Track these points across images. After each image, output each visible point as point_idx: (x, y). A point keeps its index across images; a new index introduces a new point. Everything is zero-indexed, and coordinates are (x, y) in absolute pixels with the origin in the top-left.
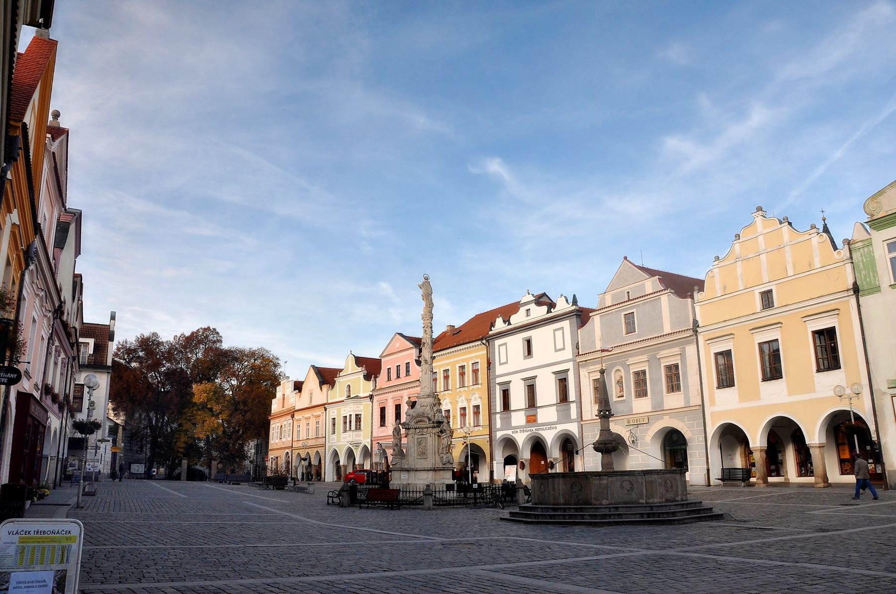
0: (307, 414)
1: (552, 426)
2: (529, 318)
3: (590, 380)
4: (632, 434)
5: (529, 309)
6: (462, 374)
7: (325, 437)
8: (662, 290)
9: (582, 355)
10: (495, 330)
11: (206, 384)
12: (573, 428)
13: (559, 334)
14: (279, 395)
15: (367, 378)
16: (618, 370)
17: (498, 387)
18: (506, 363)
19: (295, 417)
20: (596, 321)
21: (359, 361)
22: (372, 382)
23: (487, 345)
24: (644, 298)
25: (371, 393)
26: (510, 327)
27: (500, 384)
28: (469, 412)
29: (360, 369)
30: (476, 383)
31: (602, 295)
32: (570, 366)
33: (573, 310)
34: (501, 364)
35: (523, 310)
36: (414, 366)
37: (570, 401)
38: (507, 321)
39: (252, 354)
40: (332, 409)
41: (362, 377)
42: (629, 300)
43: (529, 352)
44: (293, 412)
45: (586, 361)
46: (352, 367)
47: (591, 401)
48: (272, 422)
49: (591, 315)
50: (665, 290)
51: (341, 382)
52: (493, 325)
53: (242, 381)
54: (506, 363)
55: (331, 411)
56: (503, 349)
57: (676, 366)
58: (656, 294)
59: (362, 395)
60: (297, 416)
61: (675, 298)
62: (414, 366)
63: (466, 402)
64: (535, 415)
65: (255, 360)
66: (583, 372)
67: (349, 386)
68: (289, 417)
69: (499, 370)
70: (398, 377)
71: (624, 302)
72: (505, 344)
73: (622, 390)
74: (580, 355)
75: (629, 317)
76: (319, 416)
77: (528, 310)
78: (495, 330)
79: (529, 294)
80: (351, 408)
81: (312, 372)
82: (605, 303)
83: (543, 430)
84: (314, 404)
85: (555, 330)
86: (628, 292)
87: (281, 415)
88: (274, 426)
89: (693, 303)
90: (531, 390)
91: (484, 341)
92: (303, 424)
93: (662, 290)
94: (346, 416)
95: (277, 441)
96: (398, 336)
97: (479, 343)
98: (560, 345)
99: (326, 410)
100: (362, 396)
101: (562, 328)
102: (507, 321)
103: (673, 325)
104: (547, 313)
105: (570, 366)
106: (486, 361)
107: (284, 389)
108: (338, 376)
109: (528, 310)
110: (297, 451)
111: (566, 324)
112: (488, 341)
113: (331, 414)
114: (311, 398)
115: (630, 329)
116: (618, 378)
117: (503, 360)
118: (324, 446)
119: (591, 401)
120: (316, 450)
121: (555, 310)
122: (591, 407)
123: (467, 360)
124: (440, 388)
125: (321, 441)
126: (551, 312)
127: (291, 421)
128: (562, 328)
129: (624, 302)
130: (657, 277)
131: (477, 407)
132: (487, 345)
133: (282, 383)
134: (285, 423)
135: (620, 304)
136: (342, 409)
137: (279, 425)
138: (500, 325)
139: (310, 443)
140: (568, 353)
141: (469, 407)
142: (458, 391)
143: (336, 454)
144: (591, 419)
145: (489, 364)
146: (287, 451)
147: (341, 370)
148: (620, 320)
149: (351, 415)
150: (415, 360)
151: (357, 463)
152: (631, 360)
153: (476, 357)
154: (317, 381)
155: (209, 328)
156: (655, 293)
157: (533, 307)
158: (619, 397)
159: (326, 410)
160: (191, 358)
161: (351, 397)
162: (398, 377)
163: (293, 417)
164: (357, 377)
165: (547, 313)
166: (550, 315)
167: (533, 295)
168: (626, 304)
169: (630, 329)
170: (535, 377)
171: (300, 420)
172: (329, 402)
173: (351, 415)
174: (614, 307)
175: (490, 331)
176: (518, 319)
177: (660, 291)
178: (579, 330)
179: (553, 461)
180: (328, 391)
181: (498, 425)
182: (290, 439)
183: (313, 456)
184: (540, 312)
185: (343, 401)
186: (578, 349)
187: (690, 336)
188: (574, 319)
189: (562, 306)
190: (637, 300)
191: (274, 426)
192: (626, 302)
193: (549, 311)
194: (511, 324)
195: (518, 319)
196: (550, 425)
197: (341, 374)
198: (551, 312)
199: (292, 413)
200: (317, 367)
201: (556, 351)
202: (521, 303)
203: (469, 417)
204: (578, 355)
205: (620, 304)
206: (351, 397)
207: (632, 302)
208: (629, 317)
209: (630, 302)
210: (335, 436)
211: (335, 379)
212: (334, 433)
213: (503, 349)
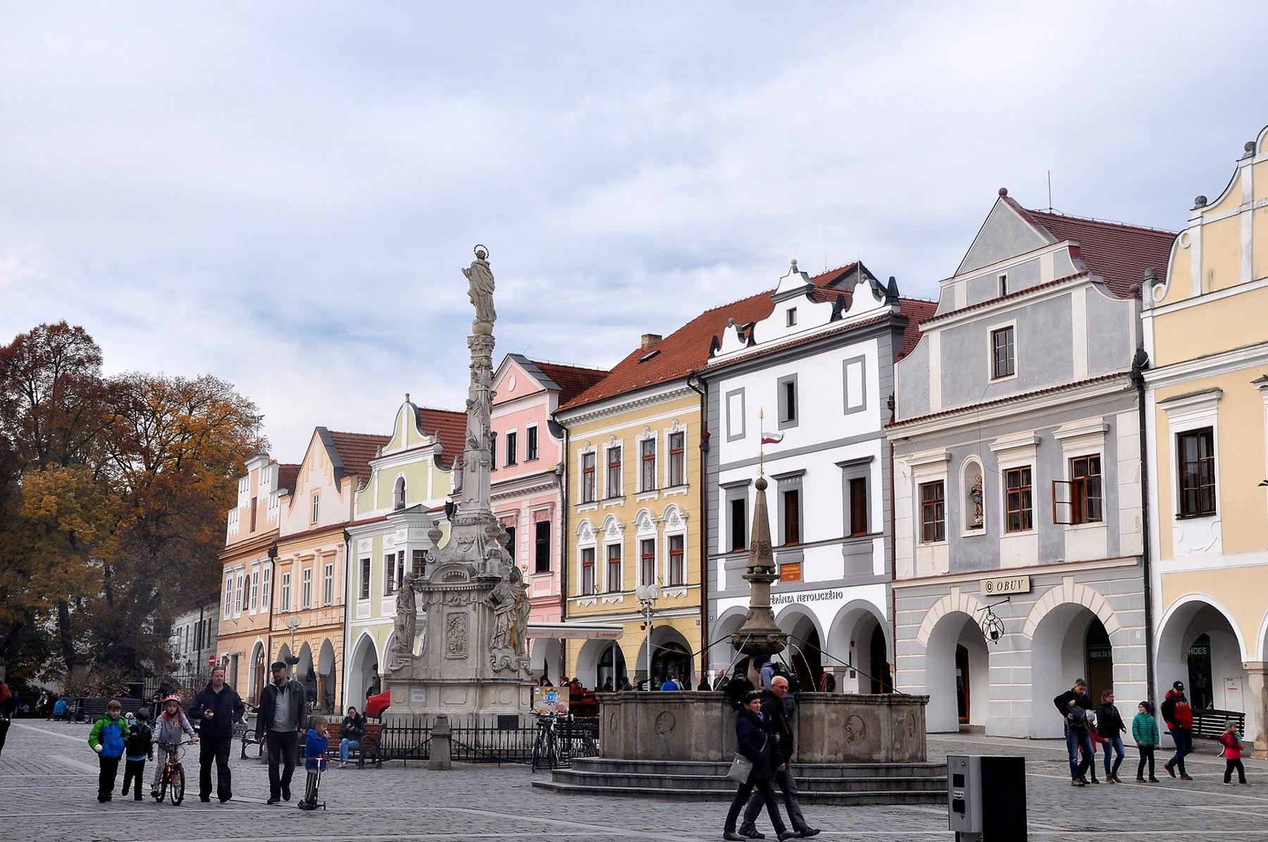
0: (307, 549)
1: (833, 590)
2: (793, 329)
3: (913, 484)
4: (991, 618)
5: (795, 309)
6: (648, 459)
7: (345, 606)
8: (1075, 277)
9: (903, 423)
10: (721, 356)
11: (55, 470)
12: (876, 596)
13: (855, 369)
14: (244, 500)
15: (442, 461)
16: (974, 466)
17: (722, 492)
18: (743, 436)
19: (279, 556)
20: (933, 343)
21: (427, 419)
22: (453, 473)
23: (704, 392)
24: (1036, 294)
25: (450, 500)
26: (753, 350)
27: (728, 486)
28: (661, 552)
29: (426, 440)
30: (676, 482)
31: (948, 282)
32: (873, 448)
33: (883, 316)
34: (730, 439)
35: (781, 309)
36: (545, 435)
37: (873, 532)
38: (746, 334)
39: (187, 393)
40: (361, 536)
41: (430, 458)
42: (1005, 297)
43: (790, 413)
44: (274, 543)
45: (906, 438)
46: (408, 435)
47: (915, 535)
48: (227, 568)
49: (922, 328)
50: (1080, 275)
51: (385, 471)
52: (716, 344)
53: (157, 464)
54: (743, 436)
55: (361, 542)
56: (736, 401)
57: (1095, 460)
58: (1063, 286)
59: (430, 503)
60: (284, 554)
61: (1104, 297)
62: (545, 435)
63: (654, 526)
64: (799, 564)
65: (192, 409)
66: (902, 466)
67: (402, 483)
68: (265, 556)
69: (727, 452)
70: (511, 461)
71: (993, 301)
72: (741, 391)
73: (979, 514)
74: (898, 424)
75: (1001, 337)
76: (334, 553)
77: (791, 312)
78: (721, 356)
79: (796, 271)
80: (401, 535)
81: (319, 442)
82: (952, 300)
83: (814, 598)
84: (322, 523)
85: (846, 363)
86: (1004, 278)
87: (247, 550)
88: (230, 576)
89: (1140, 310)
90: (792, 501)
91: (695, 383)
92: (296, 571)
93: (1075, 277)
94: (393, 556)
95: (237, 615)
96: (513, 363)
97: (684, 386)
98: (855, 400)
99: (347, 537)
100: (432, 507)
101: (861, 359)
102: (746, 334)
103: (1093, 361)
104: (832, 320)
105: (873, 448)
106: (699, 432)
107: (255, 488)
108: (377, 456)
109: (791, 312)
110: (282, 641)
111: (870, 348)
112: (704, 383)
113: (360, 549)
114: (316, 508)
115: (1002, 368)
116: (973, 483)
117: (736, 429)
118: (343, 626)
119: (915, 535)
120: (324, 636)
121: (850, 313)
122: (915, 549)
123: (660, 425)
124: (600, 491)
125: (336, 616)
126: (841, 318)
127: (269, 566)
128: (861, 359)
129: (993, 301)
130: (1067, 243)
131: (677, 540)
132: (704, 392)
133: (250, 469)
134: (256, 569)
135: (983, 304)
136: (386, 538)
137: (241, 574)
138: (731, 346)
139: (305, 621)
140: (872, 420)
141: (660, 539)
142: (638, 500)
143: (368, 648)
144: (913, 577)
145: (705, 436)
146: (259, 639)
147: (385, 441)
148: (985, 344)
149: (402, 553)
150: (548, 421)
151: (381, 671)
152: (1003, 441)
153: (677, 421)
154: (330, 467)
155: (64, 325)
156: (1058, 282)
157: (802, 302)
158: (973, 527)
159: (347, 537)
160: (16, 403)
161: (406, 508)
162: (511, 461)
163: (273, 554)
164: (420, 459)
165: (832, 320)
166: (838, 325)
167: (804, 274)
168: (997, 305)
169: (1002, 368)
170: (801, 473)
171: (291, 562)
172: (357, 518)
173: (402, 553)
174: (973, 313)
175: (709, 358)
176: (771, 332)
177: (1069, 278)
178: (896, 365)
179: (832, 673)
180: (353, 491)
181: (721, 585)
182: (266, 610)
183: (318, 653)
184: (816, 317)
185: (384, 519)
186: (893, 409)
187: (1126, 390)
188: (888, 338)
189: (865, 304)
190: (1021, 298)
191: (233, 575)
192: (998, 300)
193: (836, 316)
194: (754, 344)
195: (771, 332)
196: (829, 588)
197: (386, 451)
198: (841, 318)
199: (272, 546)
200: (331, 432)
201: (848, 411)
202: (777, 293)
203: (660, 564)
204: (892, 423)
205: (983, 304)
206: (406, 508)
207: (1011, 301)
208: (1001, 337)
209: (1007, 302)
210: (366, 603)
211: (370, 463)
212: (365, 595)
213: (736, 401)
